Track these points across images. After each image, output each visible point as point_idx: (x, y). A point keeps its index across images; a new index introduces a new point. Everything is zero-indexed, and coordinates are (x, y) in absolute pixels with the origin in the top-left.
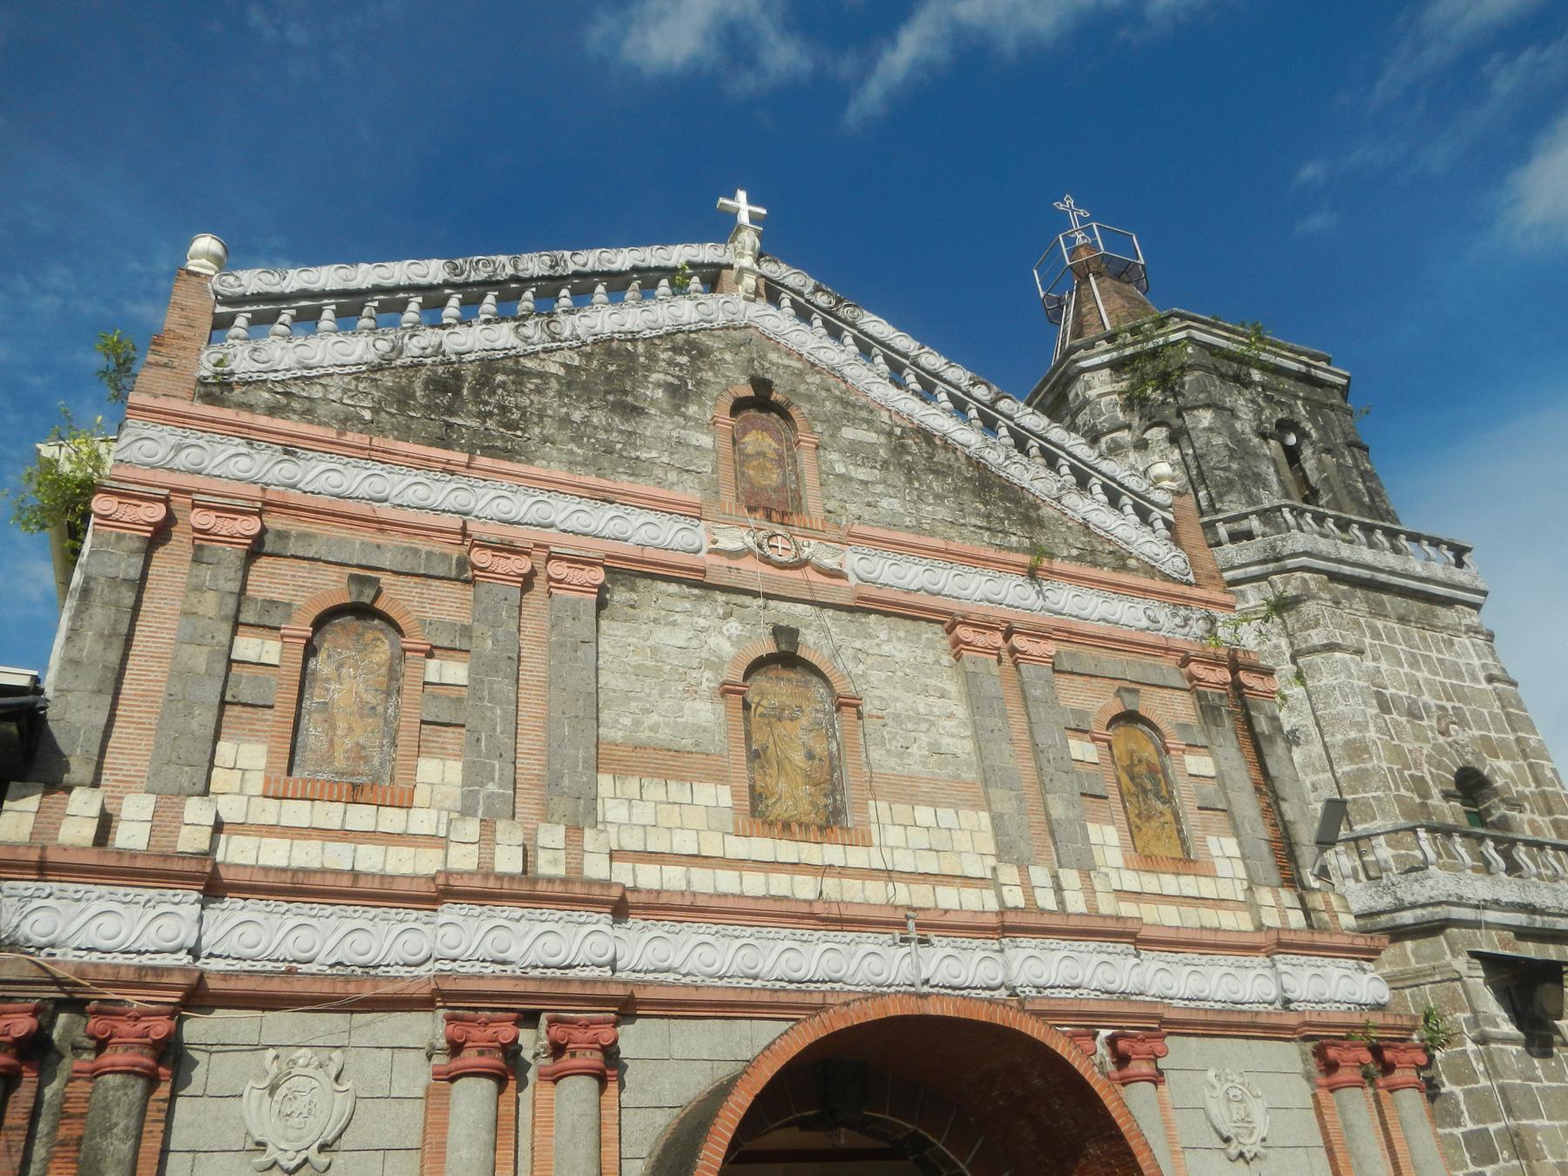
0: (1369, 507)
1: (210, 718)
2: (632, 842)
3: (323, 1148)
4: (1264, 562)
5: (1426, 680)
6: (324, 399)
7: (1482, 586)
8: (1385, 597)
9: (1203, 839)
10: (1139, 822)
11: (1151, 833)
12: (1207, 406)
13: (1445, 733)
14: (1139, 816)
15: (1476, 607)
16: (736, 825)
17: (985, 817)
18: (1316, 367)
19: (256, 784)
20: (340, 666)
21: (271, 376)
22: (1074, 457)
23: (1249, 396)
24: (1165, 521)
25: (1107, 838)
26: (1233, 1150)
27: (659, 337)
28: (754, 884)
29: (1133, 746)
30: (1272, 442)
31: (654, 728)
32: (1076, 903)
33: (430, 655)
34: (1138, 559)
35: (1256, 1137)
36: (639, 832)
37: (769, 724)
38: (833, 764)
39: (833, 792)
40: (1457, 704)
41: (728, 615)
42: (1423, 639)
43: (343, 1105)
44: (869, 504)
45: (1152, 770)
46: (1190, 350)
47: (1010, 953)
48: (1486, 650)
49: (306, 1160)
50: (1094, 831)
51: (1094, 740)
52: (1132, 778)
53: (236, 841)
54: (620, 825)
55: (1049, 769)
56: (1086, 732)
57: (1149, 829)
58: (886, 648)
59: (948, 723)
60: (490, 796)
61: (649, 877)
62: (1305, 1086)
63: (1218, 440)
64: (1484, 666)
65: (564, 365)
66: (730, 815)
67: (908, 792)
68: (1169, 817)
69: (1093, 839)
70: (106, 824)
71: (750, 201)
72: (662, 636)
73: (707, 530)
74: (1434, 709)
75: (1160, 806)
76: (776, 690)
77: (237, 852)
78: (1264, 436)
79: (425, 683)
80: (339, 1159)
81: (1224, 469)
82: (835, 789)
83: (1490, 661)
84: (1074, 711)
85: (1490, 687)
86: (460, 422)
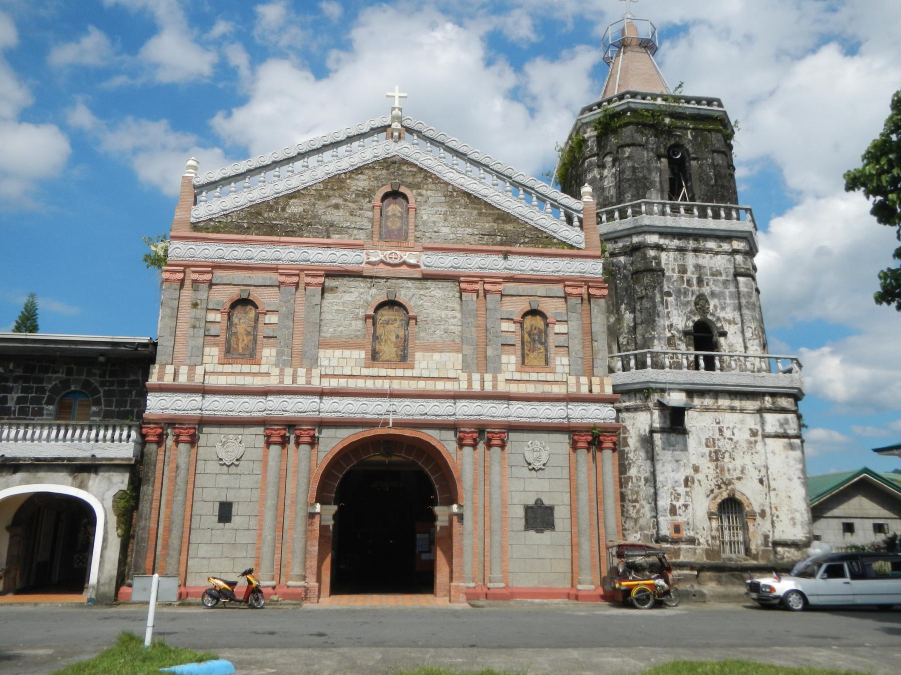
1: (202, 340)
2: (329, 371)
3: (237, 460)
6: (232, 221)
9: (554, 358)
10: (528, 353)
11: (533, 357)
14: (529, 351)
16: (365, 363)
17: (460, 355)
19: (216, 360)
20: (240, 319)
21: (214, 216)
22: (538, 193)
24: (578, 217)
25: (510, 360)
26: (530, 467)
27: (356, 169)
28: (370, 384)
29: (534, 322)
31: (341, 332)
32: (488, 387)
33: (266, 314)
34: (558, 239)
35: (542, 463)
36: (332, 368)
37: (384, 327)
38: (406, 340)
39: (405, 349)
41: (370, 288)
43: (242, 450)
44: (436, 232)
45: (540, 331)
46: (629, 114)
47: (457, 404)
49: (233, 463)
50: (504, 359)
51: (514, 323)
52: (530, 335)
53: (212, 377)
54: (326, 367)
55: (490, 336)
56: (512, 319)
57: (532, 355)
58: (433, 293)
59: (453, 320)
60: (284, 360)
61: (334, 383)
62: (568, 446)
65: (316, 190)
66: (364, 361)
67: (431, 348)
68: (543, 350)
69: (503, 361)
70: (176, 374)
71: (400, 92)
72: (347, 297)
73: (367, 254)
75: (539, 346)
76: (386, 314)
77: (212, 381)
79: (265, 324)
80: (241, 463)
82: (405, 348)
84: (507, 312)
86: (277, 223)
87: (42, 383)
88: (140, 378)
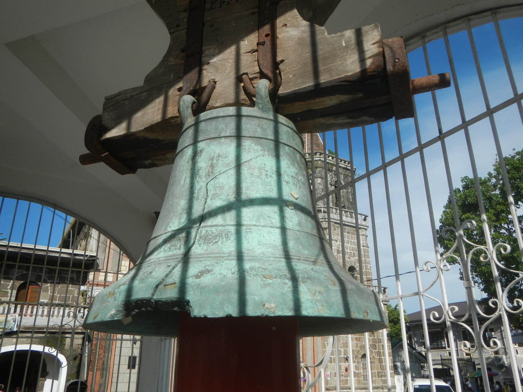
0: (351, 203)
4: (322, 219)
5: (349, 246)
7: (368, 225)
8: (346, 227)
12: (320, 178)
13: (350, 258)
15: (366, 229)
18: (348, 166)
23: (331, 174)
30: (333, 187)
40: (354, 252)
42: (352, 237)
48: (365, 239)
63: (320, 187)
64: (363, 243)
74: (349, 253)
78: (331, 185)
81: (320, 194)
83: (365, 242)
85: (363, 248)
87: (9, 275)
88: (75, 277)
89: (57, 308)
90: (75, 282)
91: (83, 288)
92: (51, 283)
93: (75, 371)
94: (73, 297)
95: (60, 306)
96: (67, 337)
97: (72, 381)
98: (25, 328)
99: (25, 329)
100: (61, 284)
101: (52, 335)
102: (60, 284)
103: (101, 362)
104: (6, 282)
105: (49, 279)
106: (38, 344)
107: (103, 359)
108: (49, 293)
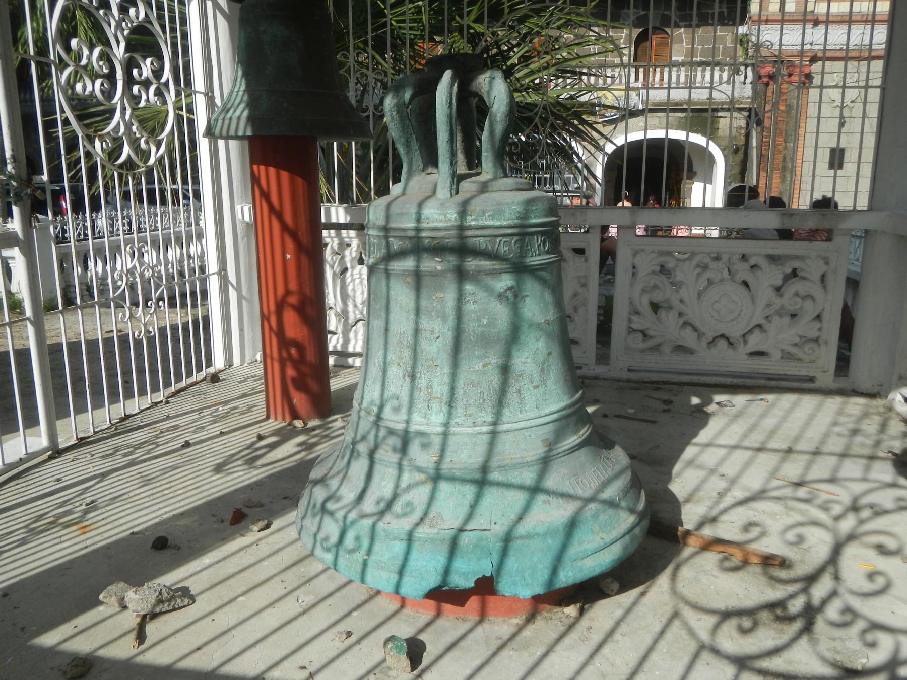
88: (725, 10)
89: (700, 69)
90: (726, 21)
91: (742, 30)
92: (686, 26)
93: (737, 170)
94: (724, 48)
95: (704, 66)
96: (720, 117)
97: (734, 185)
98: (654, 104)
99: (655, 106)
100: (702, 28)
101: (696, 115)
102: (700, 27)
103: (780, 157)
104: (616, 33)
105: (682, 20)
106: (677, 129)
107: (783, 152)
108: (684, 44)
